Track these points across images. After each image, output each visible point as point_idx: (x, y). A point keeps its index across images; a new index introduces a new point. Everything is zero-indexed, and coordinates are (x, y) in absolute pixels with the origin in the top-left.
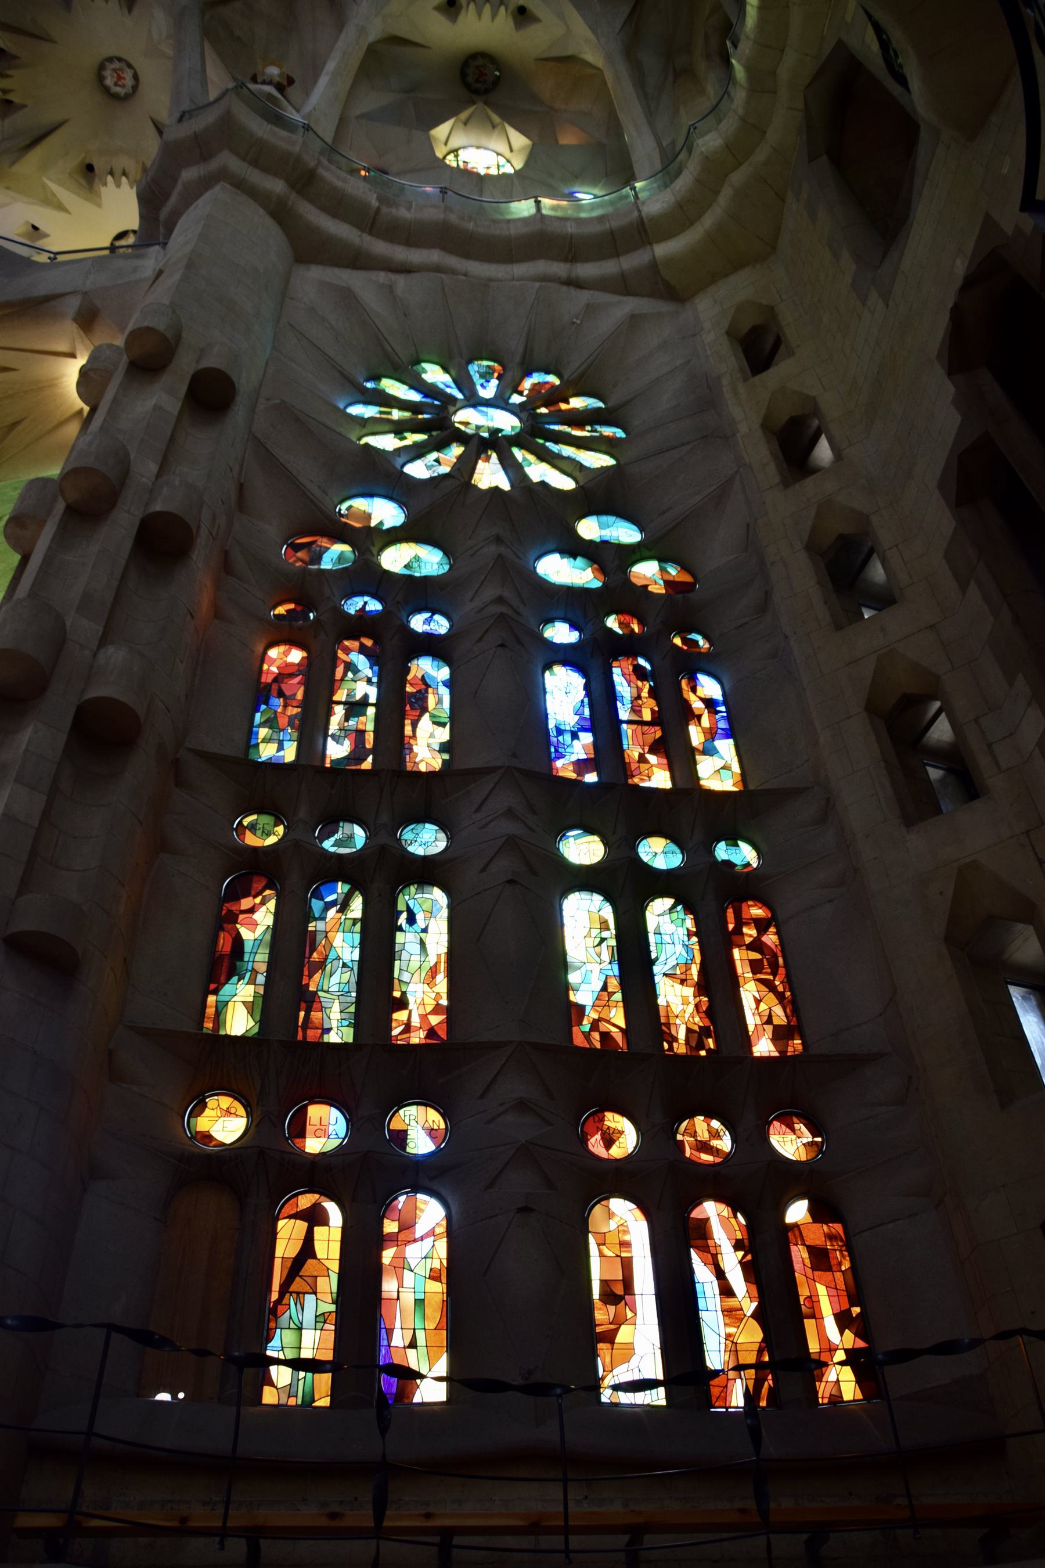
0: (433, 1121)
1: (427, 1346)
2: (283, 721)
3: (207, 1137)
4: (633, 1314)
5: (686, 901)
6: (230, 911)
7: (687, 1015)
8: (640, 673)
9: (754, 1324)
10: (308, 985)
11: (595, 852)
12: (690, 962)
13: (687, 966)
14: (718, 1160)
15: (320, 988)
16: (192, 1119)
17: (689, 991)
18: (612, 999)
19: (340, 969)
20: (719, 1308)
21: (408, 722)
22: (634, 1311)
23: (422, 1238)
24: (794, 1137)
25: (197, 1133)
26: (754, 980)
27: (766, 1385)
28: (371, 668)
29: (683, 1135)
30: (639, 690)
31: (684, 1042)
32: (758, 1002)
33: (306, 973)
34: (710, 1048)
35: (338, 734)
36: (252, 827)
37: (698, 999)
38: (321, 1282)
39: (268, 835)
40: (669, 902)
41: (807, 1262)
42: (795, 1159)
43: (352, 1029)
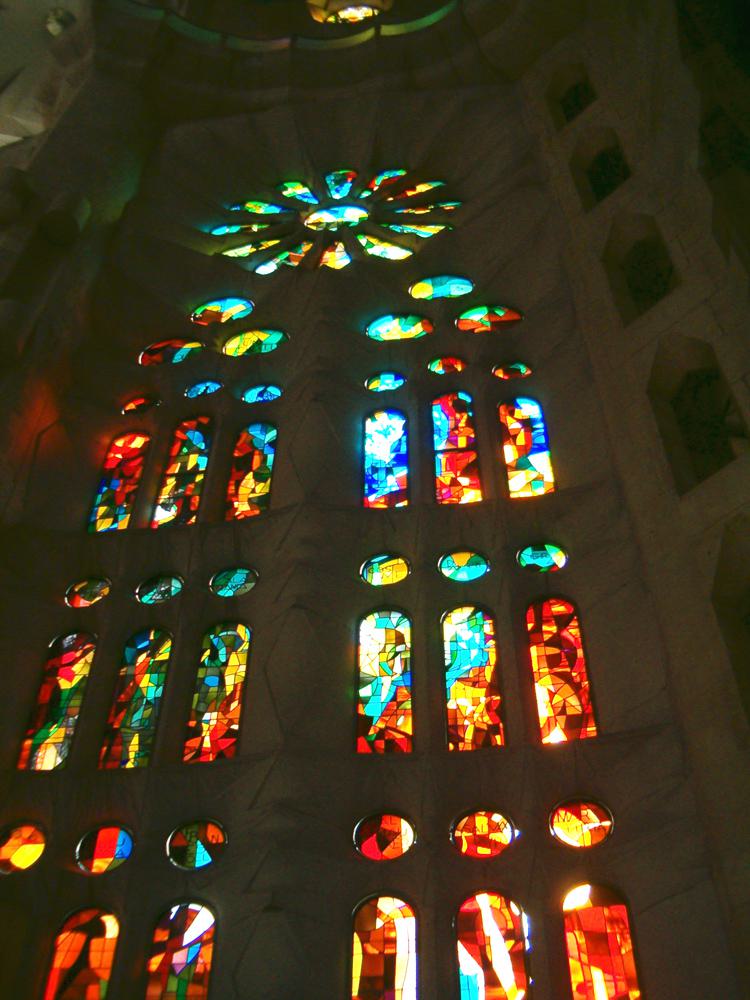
0: (213, 837)
2: (121, 497)
5: (484, 608)
6: (53, 666)
10: (112, 724)
17: (481, 693)
18: (401, 707)
19: (142, 708)
26: (550, 673)
28: (205, 441)
30: (458, 421)
32: (552, 695)
33: (113, 712)
40: (468, 611)
41: (584, 947)
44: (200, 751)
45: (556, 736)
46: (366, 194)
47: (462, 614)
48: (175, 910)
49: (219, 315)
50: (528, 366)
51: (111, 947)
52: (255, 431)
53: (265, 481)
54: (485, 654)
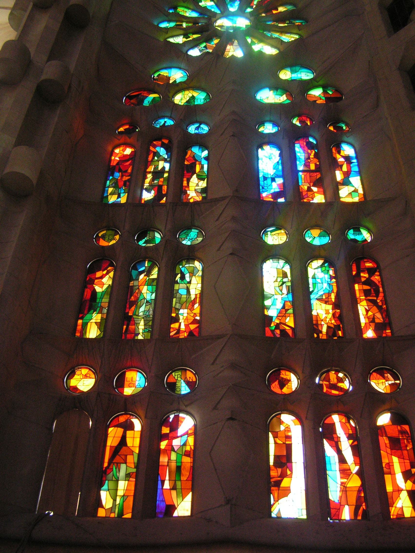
0: (190, 377)
1: (181, 489)
3: (75, 388)
4: (291, 473)
7: (328, 320)
8: (310, 146)
9: (356, 477)
10: (128, 313)
11: (281, 238)
12: (331, 292)
13: (329, 294)
14: (341, 393)
15: (134, 314)
16: (68, 381)
17: (330, 307)
19: (144, 305)
20: (338, 469)
21: (185, 179)
22: (291, 470)
23: (181, 436)
24: (384, 381)
25: (71, 387)
27: (361, 508)
28: (167, 154)
29: (323, 381)
30: (309, 155)
31: (325, 333)
32: (367, 311)
33: (128, 306)
34: (340, 336)
35: (149, 188)
36: (103, 237)
37: (334, 311)
38: (130, 458)
39: (111, 240)
40: (320, 262)
41: (388, 445)
42: (383, 392)
43: (150, 333)
44: (179, 331)
45: (370, 334)
46: (249, 10)
47: (317, 263)
48: (172, 416)
49: (168, 78)
50: (347, 125)
51: (138, 435)
52: (196, 150)
53: (203, 179)
54: (331, 286)
